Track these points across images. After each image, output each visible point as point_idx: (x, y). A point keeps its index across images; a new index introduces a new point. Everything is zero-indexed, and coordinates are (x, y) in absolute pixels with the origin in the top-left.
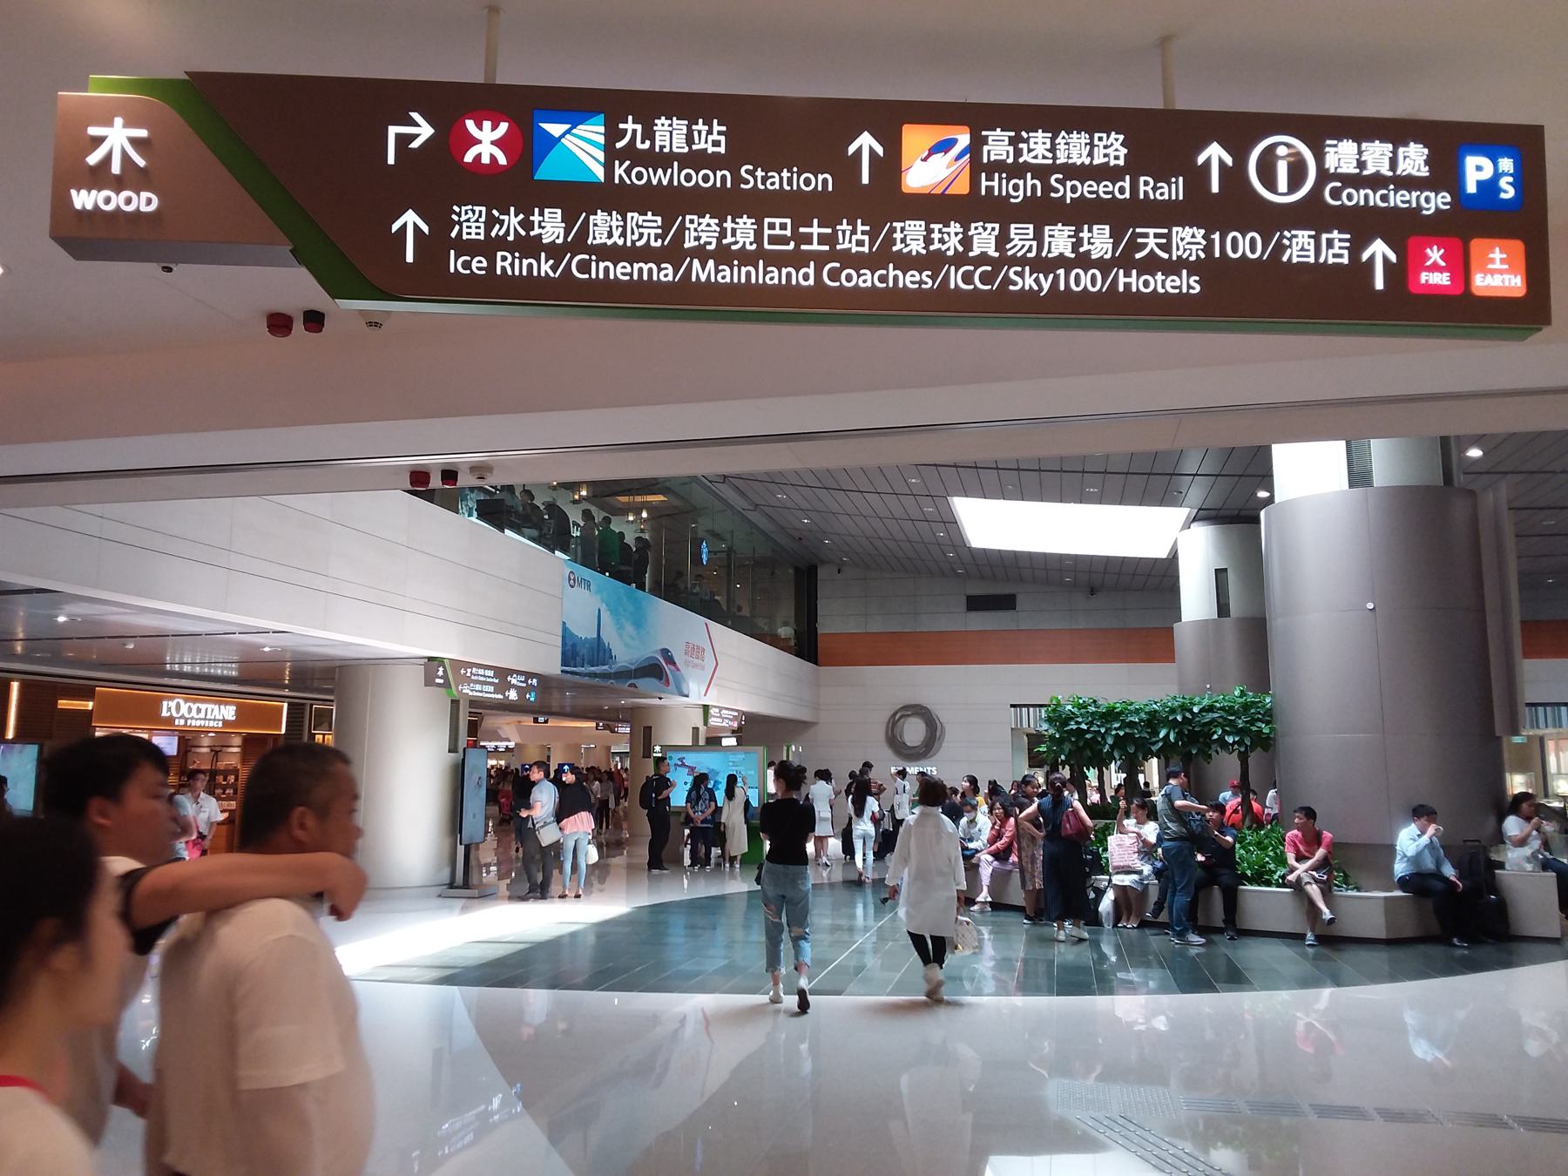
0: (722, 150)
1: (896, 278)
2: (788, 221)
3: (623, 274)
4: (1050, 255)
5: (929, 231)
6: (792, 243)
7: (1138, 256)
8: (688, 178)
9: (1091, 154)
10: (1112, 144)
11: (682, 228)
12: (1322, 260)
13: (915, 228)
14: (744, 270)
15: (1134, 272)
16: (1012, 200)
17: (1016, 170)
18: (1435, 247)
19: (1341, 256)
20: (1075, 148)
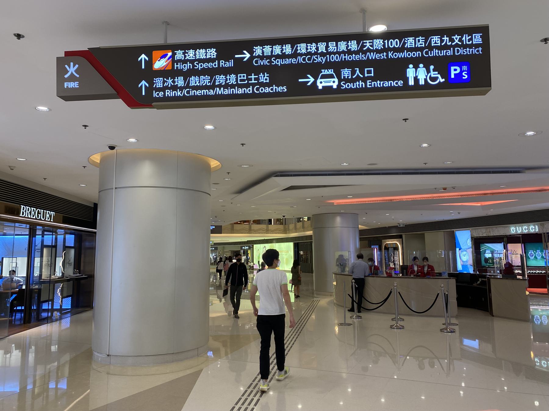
1: (276, 89)
2: (245, 75)
6: (246, 81)
11: (215, 79)
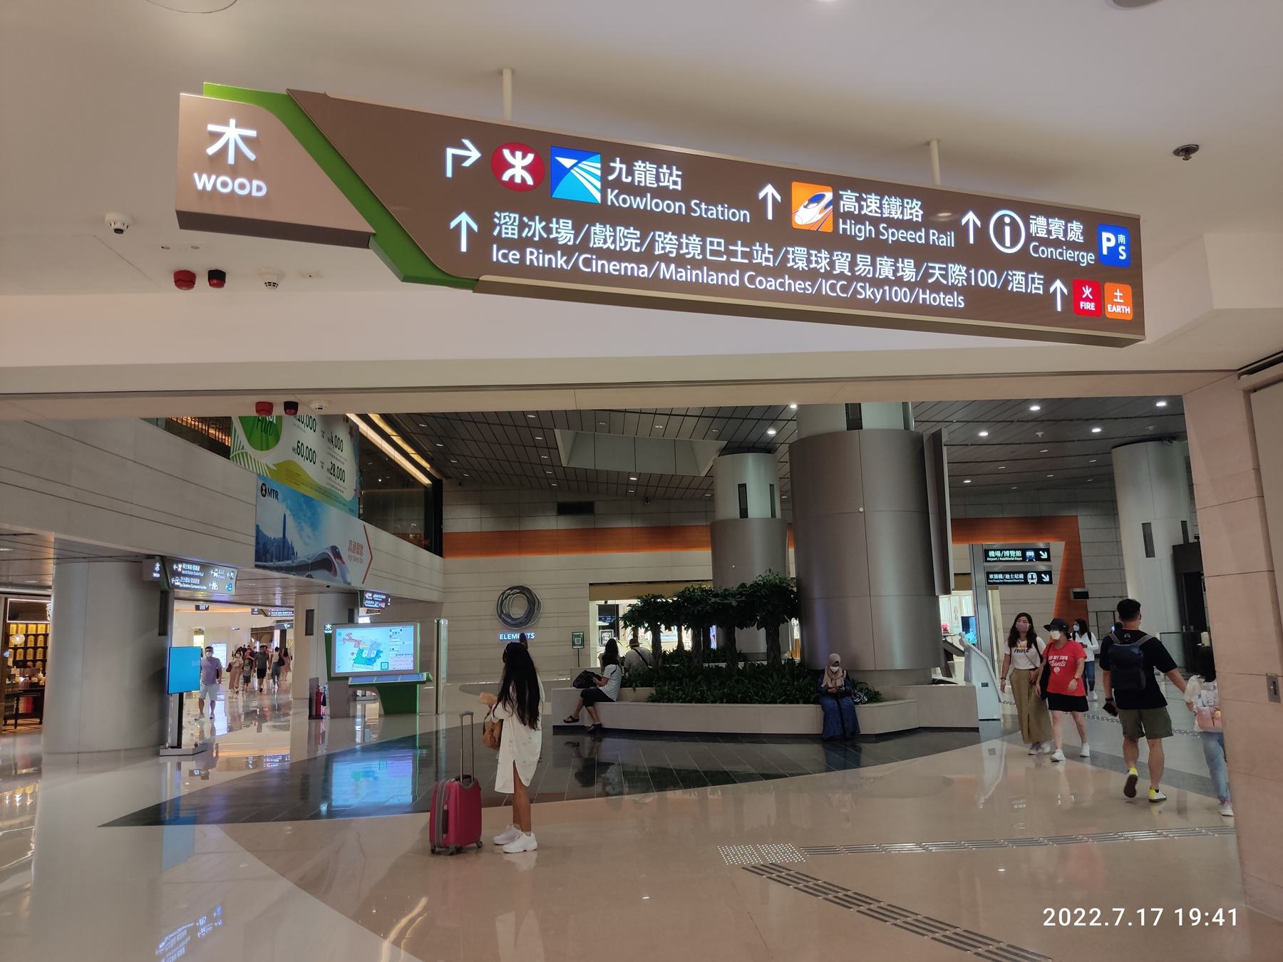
0: (679, 188)
3: (614, 270)
4: (881, 277)
5: (809, 255)
7: (930, 281)
8: (657, 205)
9: (902, 213)
10: (914, 207)
12: (1029, 291)
13: (801, 251)
14: (694, 273)
15: (928, 291)
16: (858, 239)
17: (860, 219)
18: (1087, 287)
19: (1039, 289)
20: (893, 208)
